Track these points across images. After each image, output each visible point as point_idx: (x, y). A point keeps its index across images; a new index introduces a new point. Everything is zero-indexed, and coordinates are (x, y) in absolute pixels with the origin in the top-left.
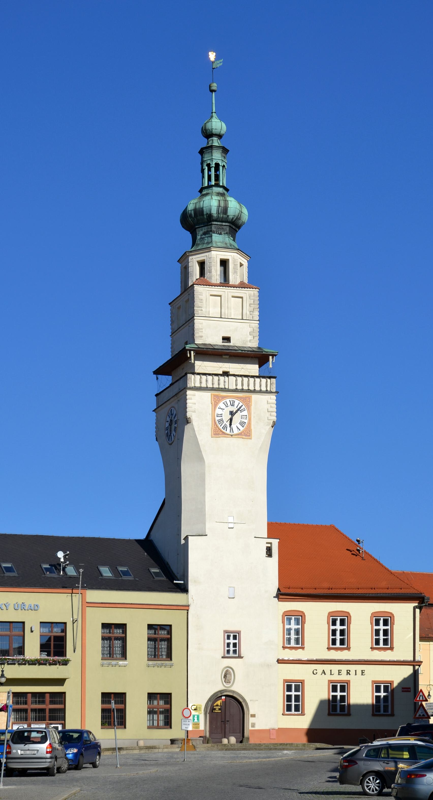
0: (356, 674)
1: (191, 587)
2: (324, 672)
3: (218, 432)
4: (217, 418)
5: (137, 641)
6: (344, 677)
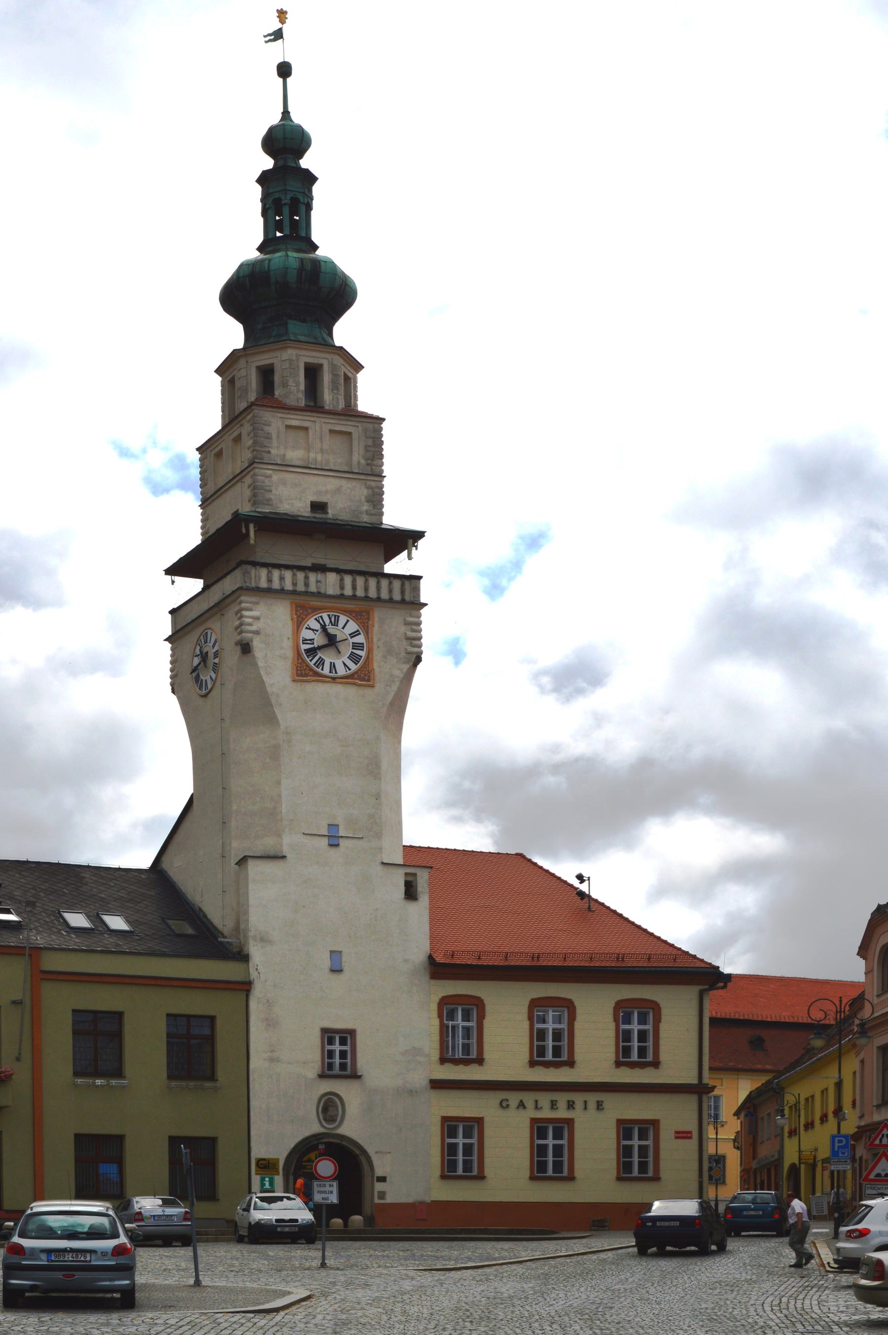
0: (586, 1108)
1: (256, 952)
2: (522, 1105)
3: (305, 670)
4: (304, 647)
5: (146, 1046)
6: (562, 1113)
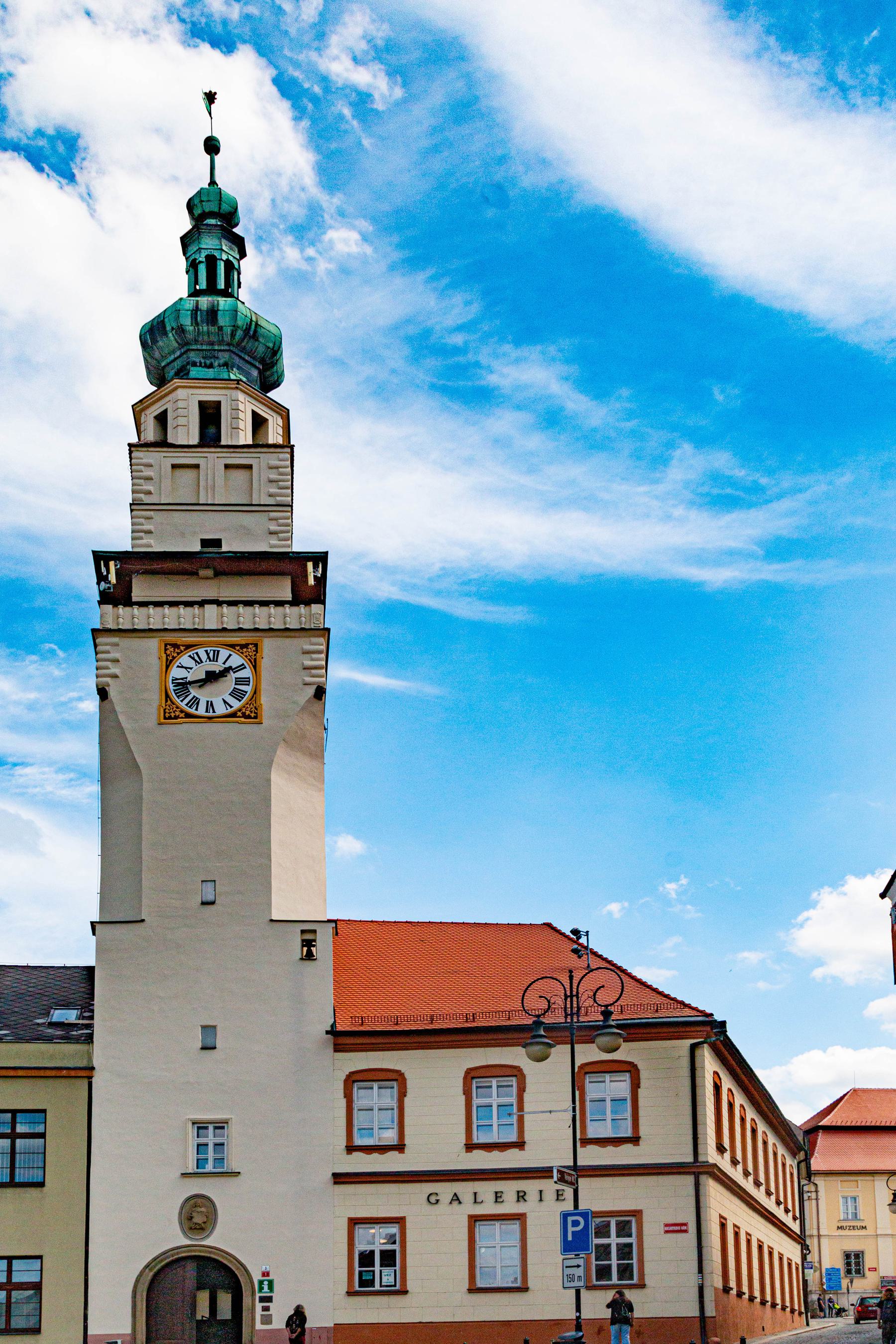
0: (541, 1200)
2: (456, 1199)
6: (510, 1206)
